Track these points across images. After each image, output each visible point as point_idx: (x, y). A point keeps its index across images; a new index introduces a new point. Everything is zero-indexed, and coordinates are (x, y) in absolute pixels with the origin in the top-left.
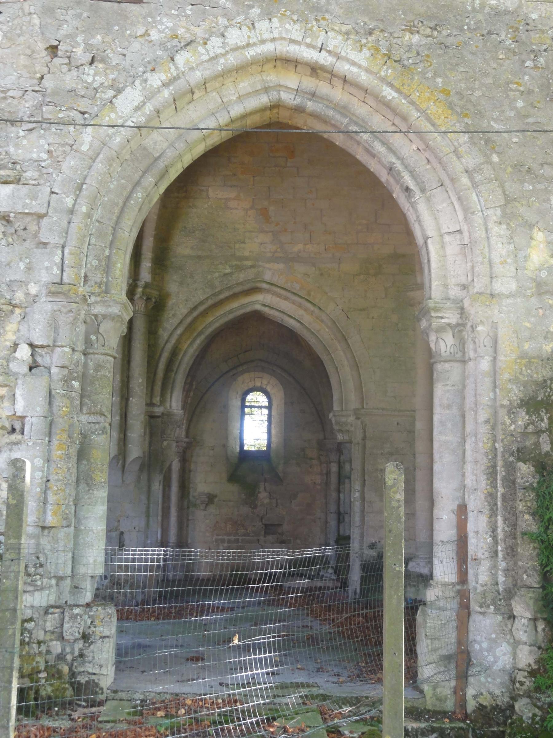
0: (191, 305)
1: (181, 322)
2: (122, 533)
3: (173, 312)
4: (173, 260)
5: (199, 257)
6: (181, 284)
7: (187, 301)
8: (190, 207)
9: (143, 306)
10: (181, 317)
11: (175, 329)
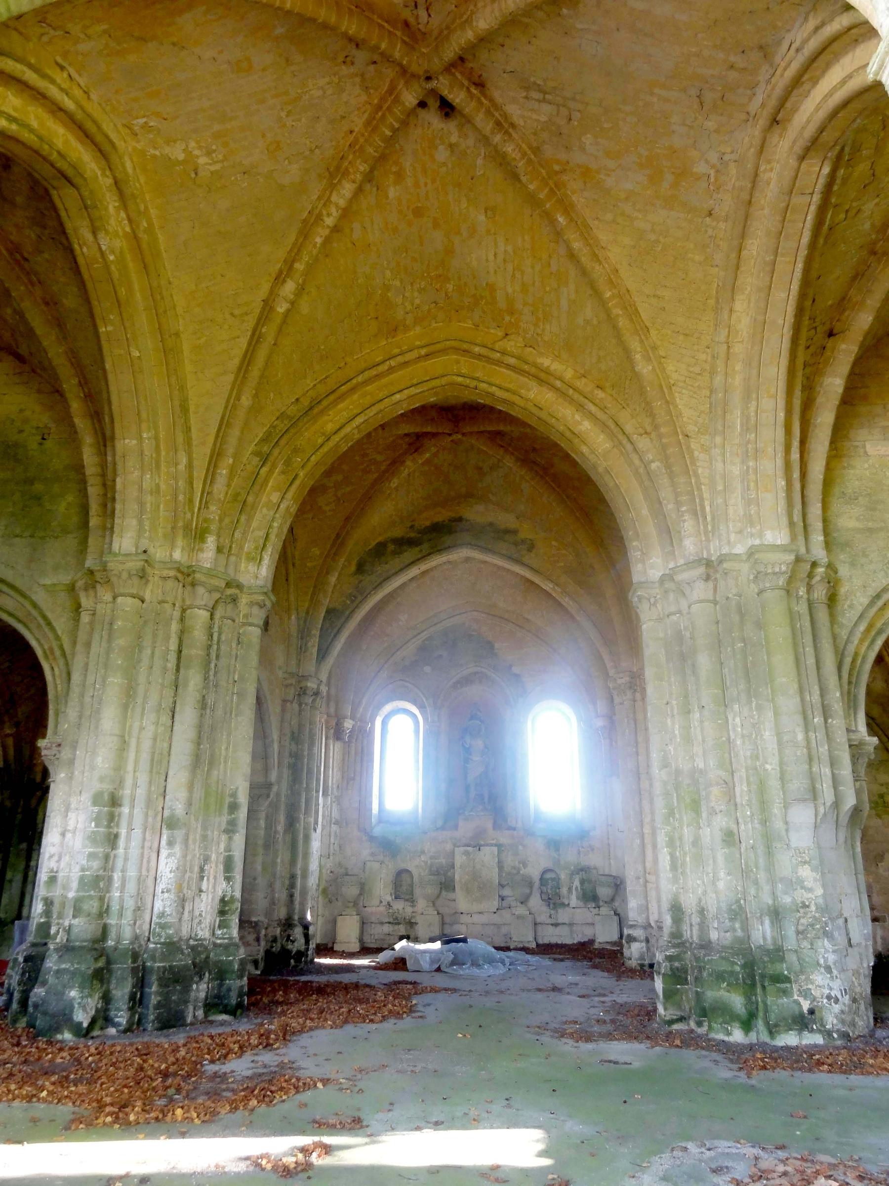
0: (871, 592)
1: (861, 616)
2: (846, 921)
3: (848, 603)
4: (835, 535)
5: (870, 530)
6: (853, 564)
7: (865, 587)
8: (844, 468)
9: (824, 592)
10: (860, 609)
11: (856, 625)
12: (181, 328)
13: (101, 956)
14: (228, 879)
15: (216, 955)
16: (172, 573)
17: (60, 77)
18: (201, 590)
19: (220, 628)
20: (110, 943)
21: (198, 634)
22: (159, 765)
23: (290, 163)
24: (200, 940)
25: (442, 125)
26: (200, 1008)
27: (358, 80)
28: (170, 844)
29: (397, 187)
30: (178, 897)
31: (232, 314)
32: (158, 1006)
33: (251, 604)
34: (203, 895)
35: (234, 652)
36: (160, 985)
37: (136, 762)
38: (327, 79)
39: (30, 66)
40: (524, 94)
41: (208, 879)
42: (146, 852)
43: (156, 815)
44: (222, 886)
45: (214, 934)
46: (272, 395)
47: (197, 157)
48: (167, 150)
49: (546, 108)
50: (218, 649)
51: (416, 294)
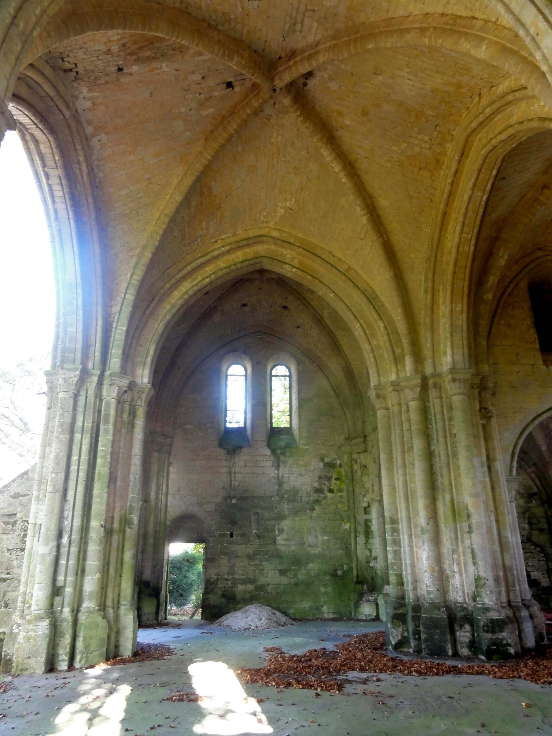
12: (350, 264)
13: (401, 607)
14: (475, 564)
15: (476, 615)
16: (391, 389)
17: (216, 246)
18: (407, 391)
19: (434, 405)
20: (407, 600)
21: (414, 416)
22: (409, 498)
23: (308, 167)
24: (459, 603)
25: (318, 78)
26: (463, 647)
27: (280, 115)
28: (423, 543)
29: (346, 118)
30: (432, 575)
31: (361, 239)
32: (426, 640)
33: (449, 382)
34: (457, 576)
35: (446, 417)
36: (425, 628)
37: (400, 498)
38: (275, 131)
39: (201, 257)
40: (298, 33)
41: (459, 564)
42: (415, 548)
43: (416, 527)
44: (471, 569)
45: (475, 600)
46: (412, 255)
47: (286, 205)
48: (279, 214)
49: (307, 22)
50: (436, 419)
51: (420, 137)
